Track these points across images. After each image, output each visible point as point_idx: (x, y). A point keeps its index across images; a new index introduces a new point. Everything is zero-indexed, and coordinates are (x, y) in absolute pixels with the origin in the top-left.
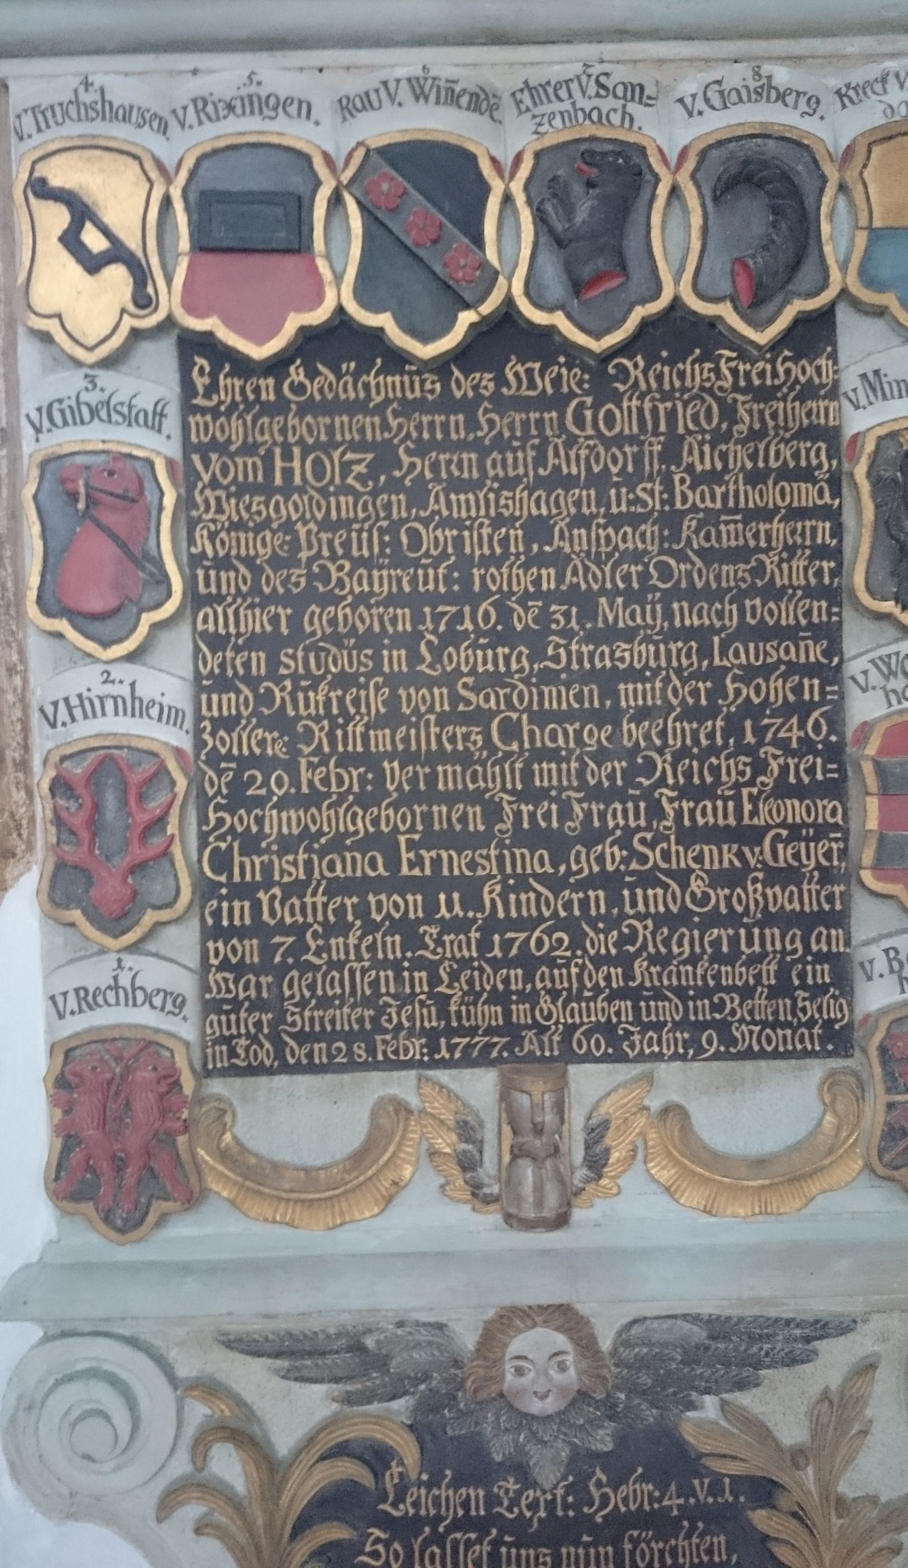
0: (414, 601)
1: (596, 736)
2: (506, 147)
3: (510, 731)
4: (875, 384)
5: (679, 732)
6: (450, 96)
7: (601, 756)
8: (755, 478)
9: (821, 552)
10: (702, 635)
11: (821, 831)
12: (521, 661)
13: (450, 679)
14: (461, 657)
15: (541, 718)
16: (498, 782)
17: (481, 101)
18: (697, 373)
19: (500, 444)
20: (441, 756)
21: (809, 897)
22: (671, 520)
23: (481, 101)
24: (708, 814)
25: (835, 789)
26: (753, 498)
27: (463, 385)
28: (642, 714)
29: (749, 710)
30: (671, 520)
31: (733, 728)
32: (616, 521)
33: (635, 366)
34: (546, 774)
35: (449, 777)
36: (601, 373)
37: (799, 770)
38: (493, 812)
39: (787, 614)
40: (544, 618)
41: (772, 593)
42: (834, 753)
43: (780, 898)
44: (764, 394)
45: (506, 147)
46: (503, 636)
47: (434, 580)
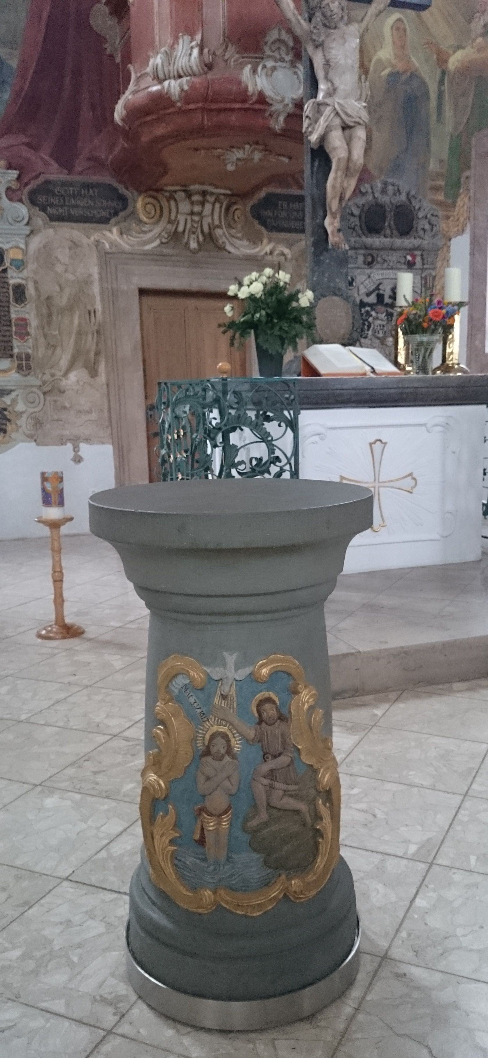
4: (12, 277)
9: (7, 297)
11: (9, 331)
21: (7, 339)
25: (10, 326)
37: (5, 323)
42: (10, 321)
43: (4, 339)
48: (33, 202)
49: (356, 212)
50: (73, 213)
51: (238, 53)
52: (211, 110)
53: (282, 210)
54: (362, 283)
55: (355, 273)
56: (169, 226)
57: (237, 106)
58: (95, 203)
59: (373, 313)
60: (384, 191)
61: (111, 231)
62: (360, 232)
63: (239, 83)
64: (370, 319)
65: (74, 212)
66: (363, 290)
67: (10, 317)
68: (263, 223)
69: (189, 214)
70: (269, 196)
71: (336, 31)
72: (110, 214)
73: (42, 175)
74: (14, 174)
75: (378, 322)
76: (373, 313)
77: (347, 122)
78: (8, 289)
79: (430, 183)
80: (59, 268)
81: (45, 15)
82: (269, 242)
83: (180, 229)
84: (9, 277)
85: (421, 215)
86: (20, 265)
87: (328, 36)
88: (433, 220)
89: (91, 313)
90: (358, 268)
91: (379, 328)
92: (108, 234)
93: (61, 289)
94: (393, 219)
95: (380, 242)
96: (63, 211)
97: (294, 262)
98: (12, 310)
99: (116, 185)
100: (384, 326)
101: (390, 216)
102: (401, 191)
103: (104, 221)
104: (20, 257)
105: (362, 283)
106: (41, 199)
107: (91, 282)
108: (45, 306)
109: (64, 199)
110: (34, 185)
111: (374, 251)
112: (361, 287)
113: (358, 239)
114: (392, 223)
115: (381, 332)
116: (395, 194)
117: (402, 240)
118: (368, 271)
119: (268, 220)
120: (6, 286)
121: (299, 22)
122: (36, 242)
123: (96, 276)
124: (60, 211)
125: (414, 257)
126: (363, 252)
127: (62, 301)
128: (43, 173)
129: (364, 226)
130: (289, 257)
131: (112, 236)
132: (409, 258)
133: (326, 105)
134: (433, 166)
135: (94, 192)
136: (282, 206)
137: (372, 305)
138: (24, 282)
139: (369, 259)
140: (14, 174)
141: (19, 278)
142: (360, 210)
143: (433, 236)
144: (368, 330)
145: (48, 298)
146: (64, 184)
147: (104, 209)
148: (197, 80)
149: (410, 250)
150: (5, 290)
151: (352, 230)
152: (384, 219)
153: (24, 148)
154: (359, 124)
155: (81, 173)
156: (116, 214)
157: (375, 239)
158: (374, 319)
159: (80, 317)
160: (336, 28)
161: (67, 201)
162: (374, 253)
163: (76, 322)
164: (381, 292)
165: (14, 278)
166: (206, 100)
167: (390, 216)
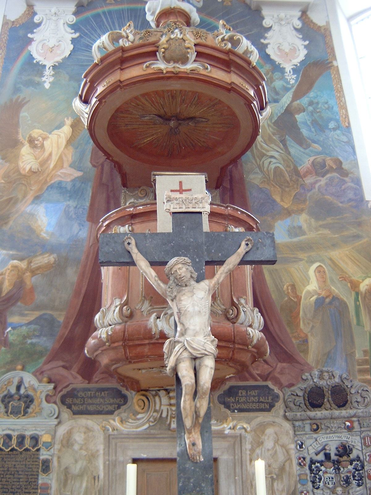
0: (4, 471)
1: (18, 483)
2: (15, 434)
3: (11, 483)
4: (43, 454)
5: (25, 483)
6: (11, 430)
7: (18, 485)
8: (33, 462)
10: (27, 475)
12: (12, 476)
13: (6, 478)
14: (8, 476)
15: (13, 482)
16: (9, 487)
17: (13, 430)
18: (28, 453)
19: (12, 458)
20: (4, 485)
22: (26, 465)
23: (13, 430)
24: (27, 491)
25: (37, 489)
26: (32, 463)
27: (10, 453)
28: (22, 482)
29: (31, 482)
30: (26, 465)
31: (29, 483)
32: (21, 465)
33: (24, 452)
34: (13, 487)
35: (5, 487)
36: (21, 453)
38: (9, 490)
39: (35, 473)
40: (15, 473)
41: (33, 472)
42: (38, 486)
44: (34, 455)
45: (15, 434)
46: (11, 474)
47: (6, 469)
48: (63, 402)
49: (301, 393)
50: (89, 409)
51: (151, 306)
52: (130, 347)
53: (242, 396)
54: (311, 445)
55: (304, 438)
56: (155, 414)
57: (147, 342)
58: (105, 401)
59: (323, 468)
60: (321, 377)
61: (114, 420)
62: (305, 407)
63: (146, 326)
64: (321, 473)
65: (91, 408)
66: (312, 451)
67: (38, 482)
68: (227, 406)
69: (168, 405)
70: (231, 388)
71: (186, 288)
72: (115, 408)
73: (71, 385)
74: (51, 386)
75: (327, 476)
76: (323, 468)
77: (195, 354)
78: (39, 463)
79: (357, 367)
80: (76, 447)
81: (83, 291)
82: (233, 420)
83: (164, 415)
84: (41, 454)
85: (353, 391)
86: (48, 446)
87: (179, 292)
88: (364, 394)
89: (95, 478)
90: (306, 434)
91: (328, 480)
92: (112, 422)
93: (76, 461)
94: (330, 396)
95: (322, 414)
96: (82, 407)
97: (253, 433)
98: (40, 477)
99: (120, 388)
100: (332, 478)
101: (328, 394)
102: (335, 375)
103: (111, 413)
104: (49, 440)
105: (311, 445)
106: (69, 401)
107: (98, 456)
108: (64, 474)
109: (84, 400)
110: (64, 392)
111: (318, 421)
112: (310, 448)
113: (303, 413)
114: (330, 399)
115: (330, 483)
116: (330, 378)
117: (339, 411)
118: (315, 436)
119: (231, 404)
120: (37, 460)
121: (159, 285)
122: (62, 430)
123: (101, 452)
124: (81, 408)
125: (352, 422)
126: (309, 422)
127: (76, 469)
128: (72, 384)
129: (307, 403)
130: (249, 429)
131: (115, 422)
132: (348, 424)
133: (179, 342)
134: (359, 355)
135: (105, 394)
136: (242, 394)
137: (321, 463)
138: (50, 458)
139: (315, 427)
140: (51, 386)
141: (47, 455)
142: (303, 392)
143: (366, 406)
144: (320, 482)
145: (66, 468)
146: (85, 390)
147: (111, 404)
148: (118, 327)
149: (348, 417)
150: (37, 463)
151: (298, 407)
152: (323, 396)
153: (61, 368)
154: (206, 355)
155: (97, 382)
156: (119, 407)
157: (317, 412)
158: (324, 473)
159: (87, 481)
160: (186, 286)
161: (86, 401)
162: (318, 422)
163: (84, 485)
164: (328, 451)
165: (44, 455)
166: (124, 339)
167: (328, 394)
